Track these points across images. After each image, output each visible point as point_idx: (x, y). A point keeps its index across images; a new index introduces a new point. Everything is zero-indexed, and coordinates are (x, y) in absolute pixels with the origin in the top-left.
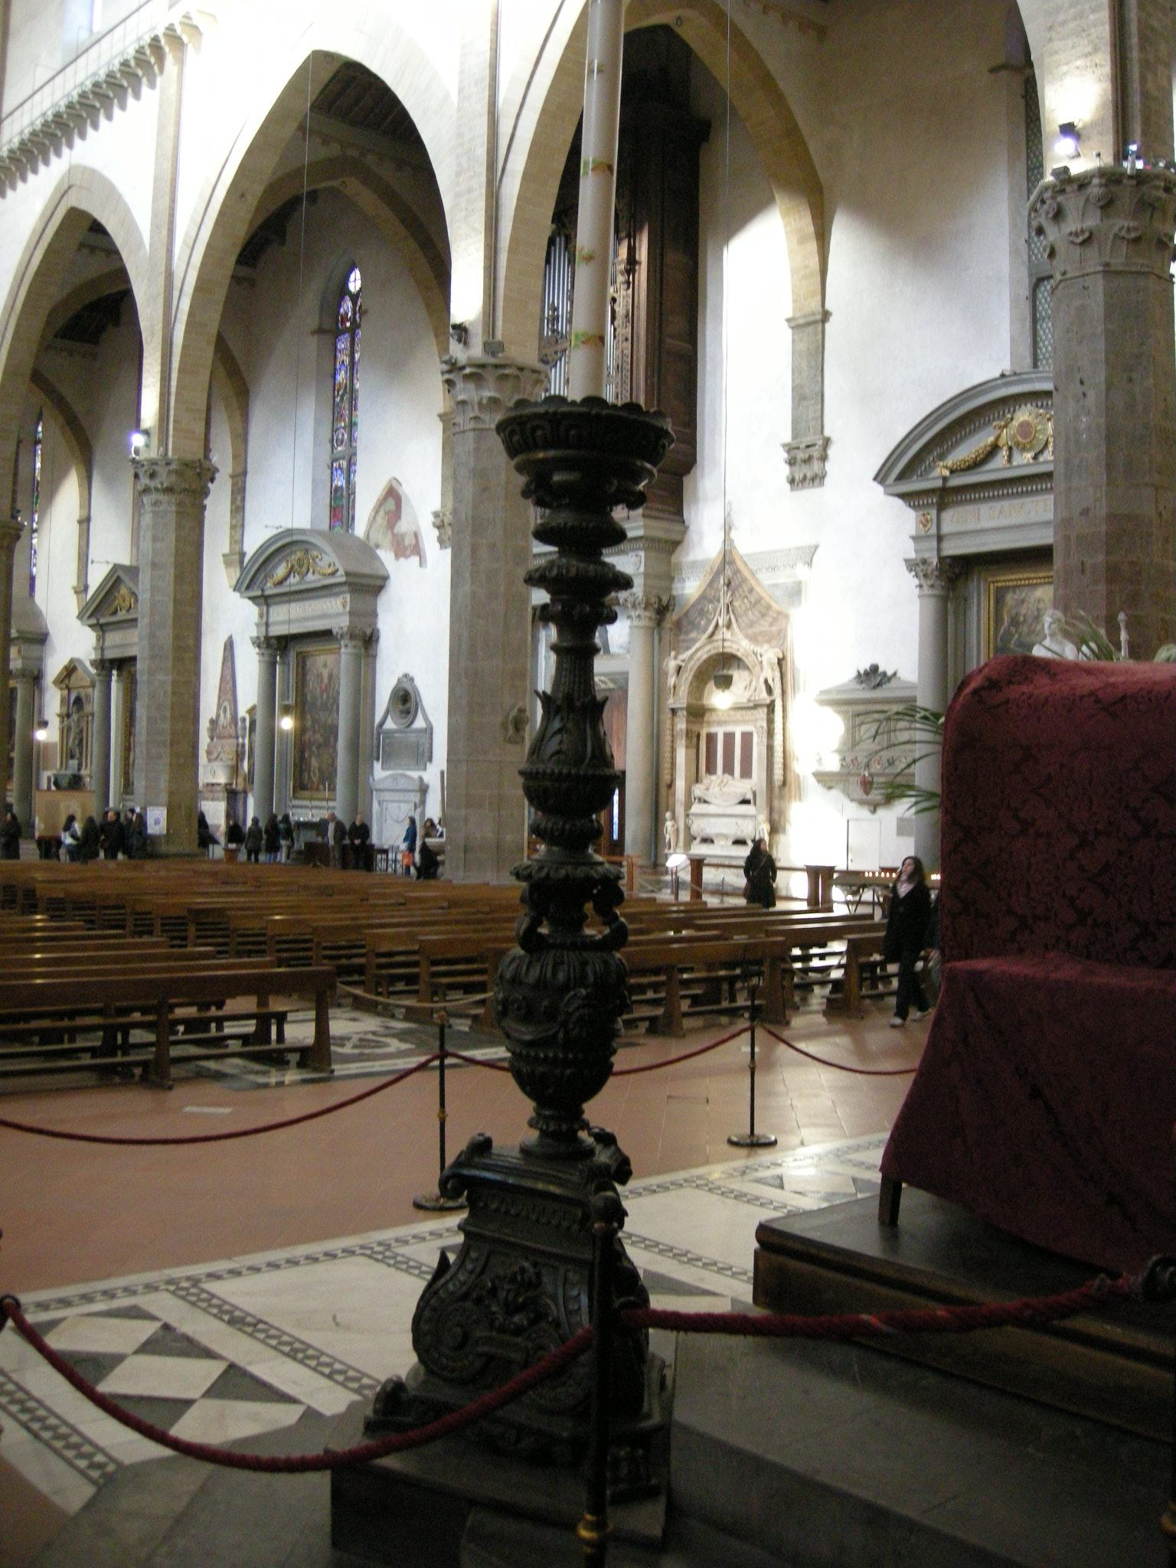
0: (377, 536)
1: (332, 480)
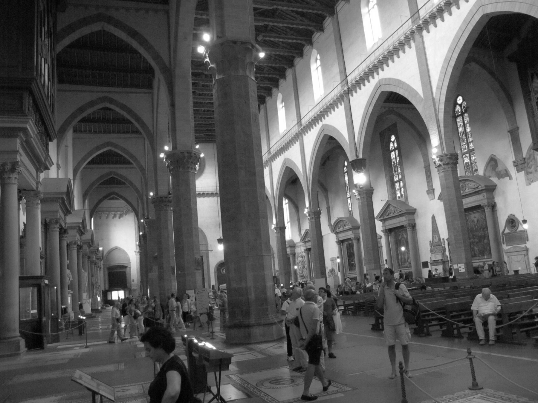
0: (488, 174)
1: (464, 161)
